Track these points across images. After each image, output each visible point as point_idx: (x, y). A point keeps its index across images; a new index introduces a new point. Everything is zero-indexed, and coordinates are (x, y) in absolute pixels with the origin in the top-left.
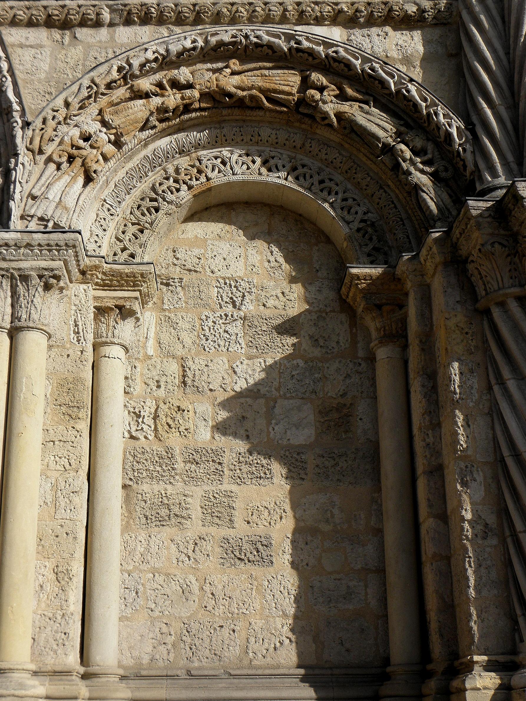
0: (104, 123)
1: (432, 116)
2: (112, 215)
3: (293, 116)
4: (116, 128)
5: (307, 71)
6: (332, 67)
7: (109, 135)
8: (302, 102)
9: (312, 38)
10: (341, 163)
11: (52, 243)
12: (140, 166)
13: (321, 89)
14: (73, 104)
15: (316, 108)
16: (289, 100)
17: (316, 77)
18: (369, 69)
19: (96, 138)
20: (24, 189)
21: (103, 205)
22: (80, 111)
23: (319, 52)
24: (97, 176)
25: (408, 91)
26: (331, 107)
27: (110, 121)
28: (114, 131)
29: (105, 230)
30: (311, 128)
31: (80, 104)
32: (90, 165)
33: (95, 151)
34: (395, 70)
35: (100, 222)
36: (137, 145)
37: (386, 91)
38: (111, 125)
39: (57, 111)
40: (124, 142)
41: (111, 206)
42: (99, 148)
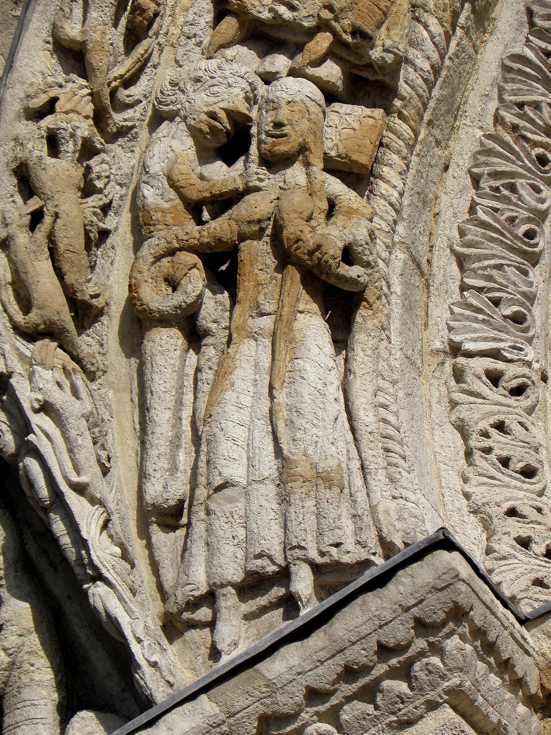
0: (264, 37)
2: (518, 391)
4: (323, 26)
7: (311, 71)
11: (359, 654)
12: (509, 117)
14: (97, 36)
19: (269, 117)
20: (112, 506)
21: (459, 375)
22: (140, 49)
24: (368, 265)
27: (282, 10)
28: (323, 41)
29: (529, 472)
31: (123, 21)
32: (310, 241)
33: (296, 174)
35: (488, 451)
36: (448, 37)
38: (293, 26)
39: (50, 107)
40: (390, 58)
41: (495, 354)
42: (303, 149)
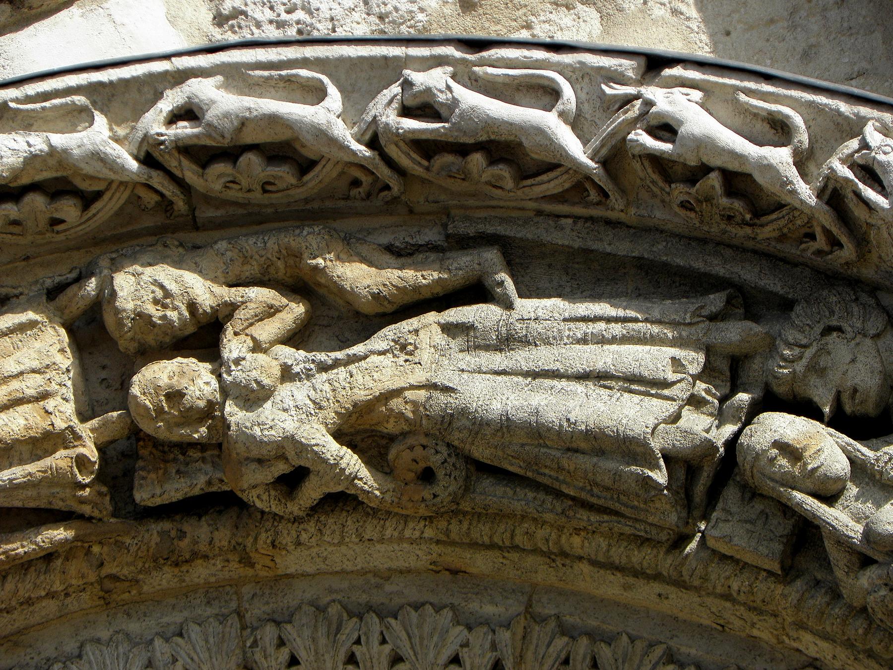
1: (858, 195)
3: (119, 545)
5: (81, 279)
6: (207, 199)
8: (129, 455)
9: (29, 99)
13: (203, 337)
15: (219, 445)
16: (55, 479)
17: (146, 287)
18: (406, 111)
23: (98, 157)
25: (666, 129)
26: (294, 402)
30: (247, 561)
34: (539, 54)
37: (551, 184)
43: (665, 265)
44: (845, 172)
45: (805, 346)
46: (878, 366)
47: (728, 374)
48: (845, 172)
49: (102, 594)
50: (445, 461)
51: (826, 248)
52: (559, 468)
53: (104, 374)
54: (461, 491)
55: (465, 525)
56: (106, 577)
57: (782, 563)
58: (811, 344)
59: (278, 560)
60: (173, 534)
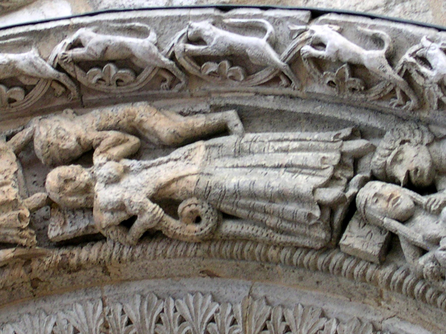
1: (418, 72)
6: (90, 90)
10: (234, 322)
13: (84, 155)
18: (189, 41)
25: (319, 44)
34: (258, 12)
43: (320, 116)
44: (412, 60)
45: (392, 150)
46: (429, 158)
47: (352, 167)
48: (412, 60)
49: (31, 289)
50: (207, 211)
51: (402, 103)
52: (265, 212)
53: (35, 179)
54: (215, 227)
55: (218, 246)
56: (34, 279)
57: (380, 260)
58: (395, 149)
59: (122, 270)
60: (68, 255)
